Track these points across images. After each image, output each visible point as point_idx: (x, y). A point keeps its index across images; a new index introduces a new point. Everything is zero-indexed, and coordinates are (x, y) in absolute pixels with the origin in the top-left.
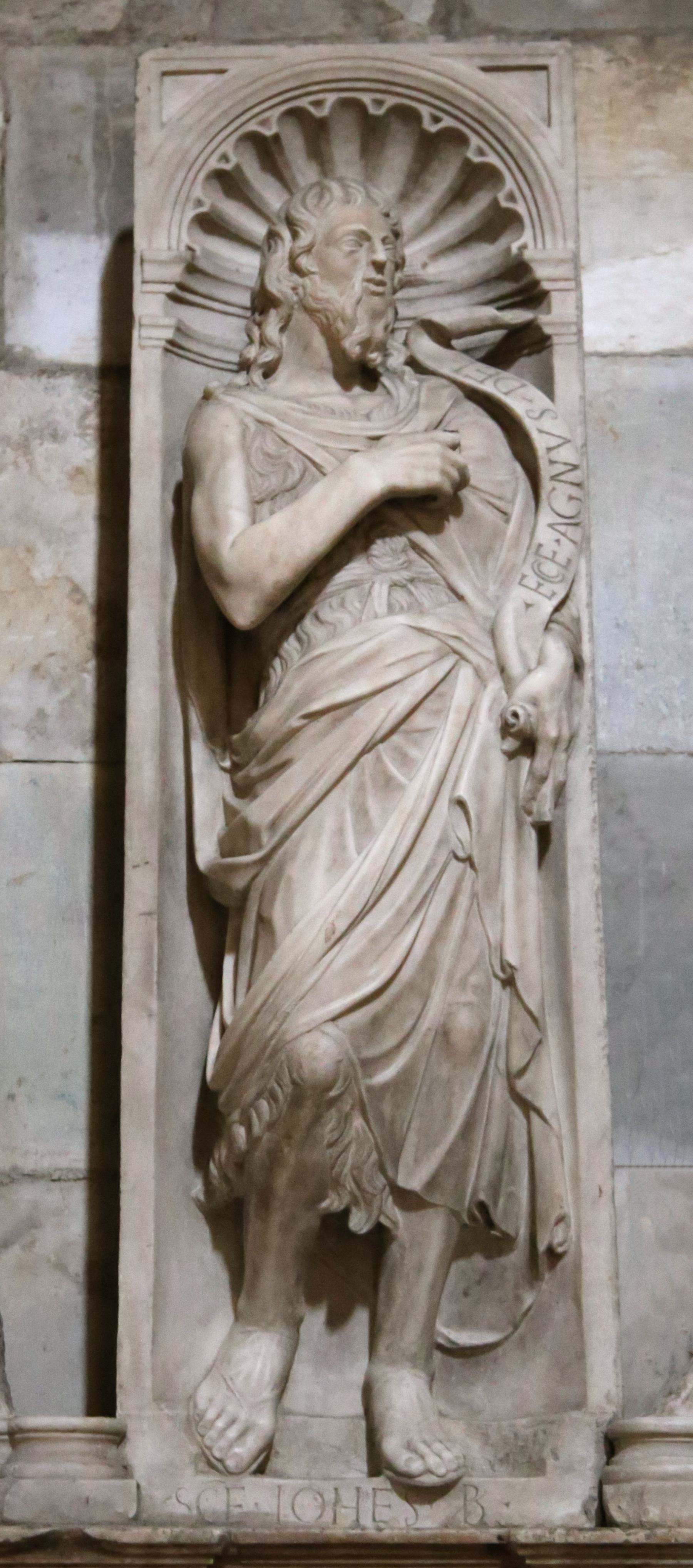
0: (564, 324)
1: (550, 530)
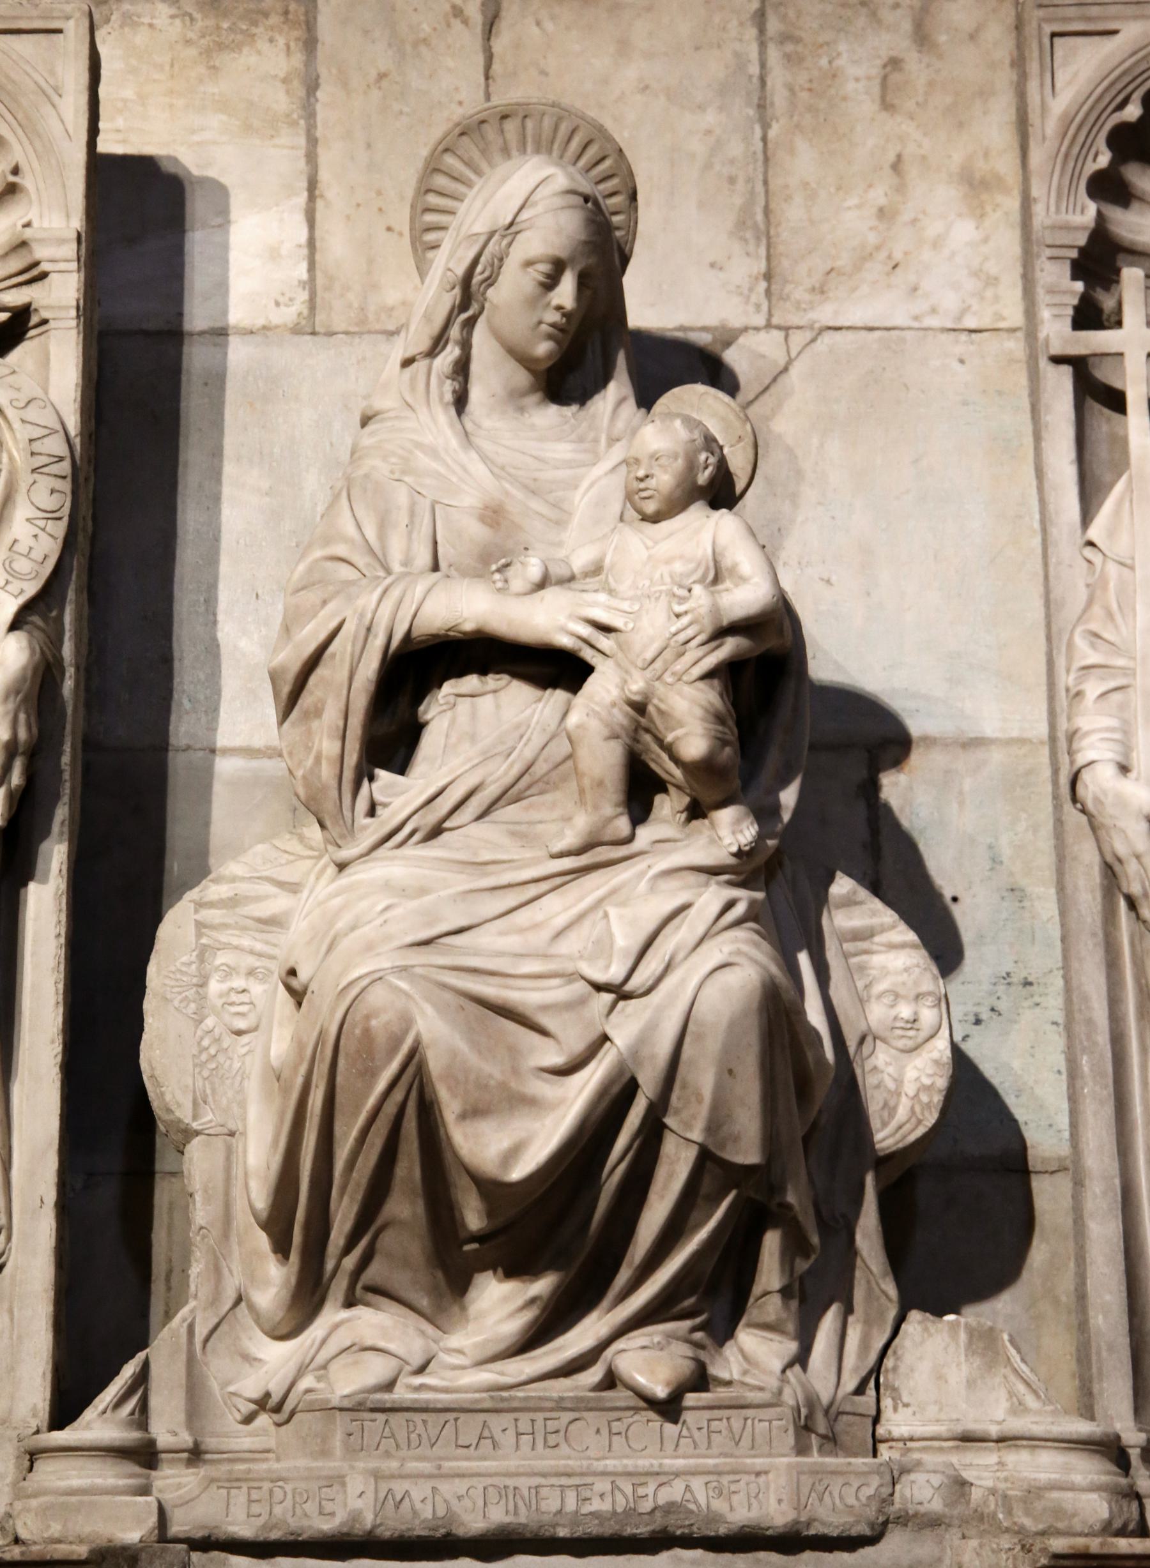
0: (60, 308)
1: (28, 524)
